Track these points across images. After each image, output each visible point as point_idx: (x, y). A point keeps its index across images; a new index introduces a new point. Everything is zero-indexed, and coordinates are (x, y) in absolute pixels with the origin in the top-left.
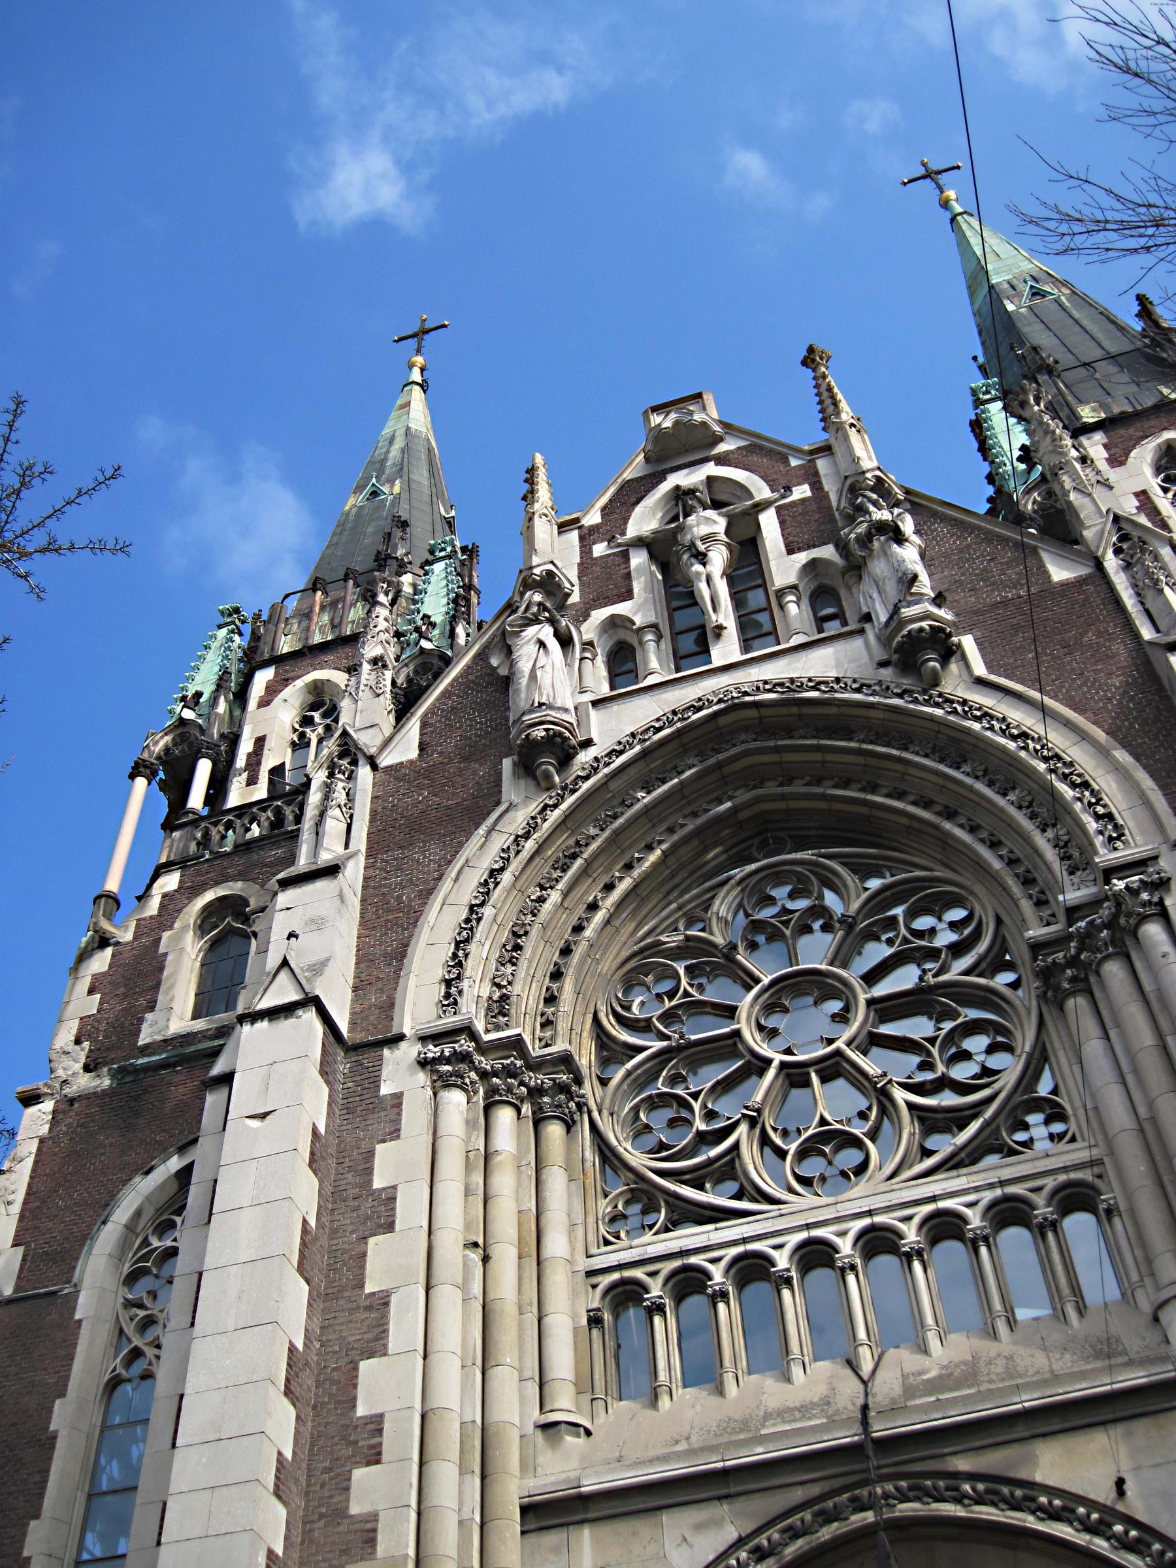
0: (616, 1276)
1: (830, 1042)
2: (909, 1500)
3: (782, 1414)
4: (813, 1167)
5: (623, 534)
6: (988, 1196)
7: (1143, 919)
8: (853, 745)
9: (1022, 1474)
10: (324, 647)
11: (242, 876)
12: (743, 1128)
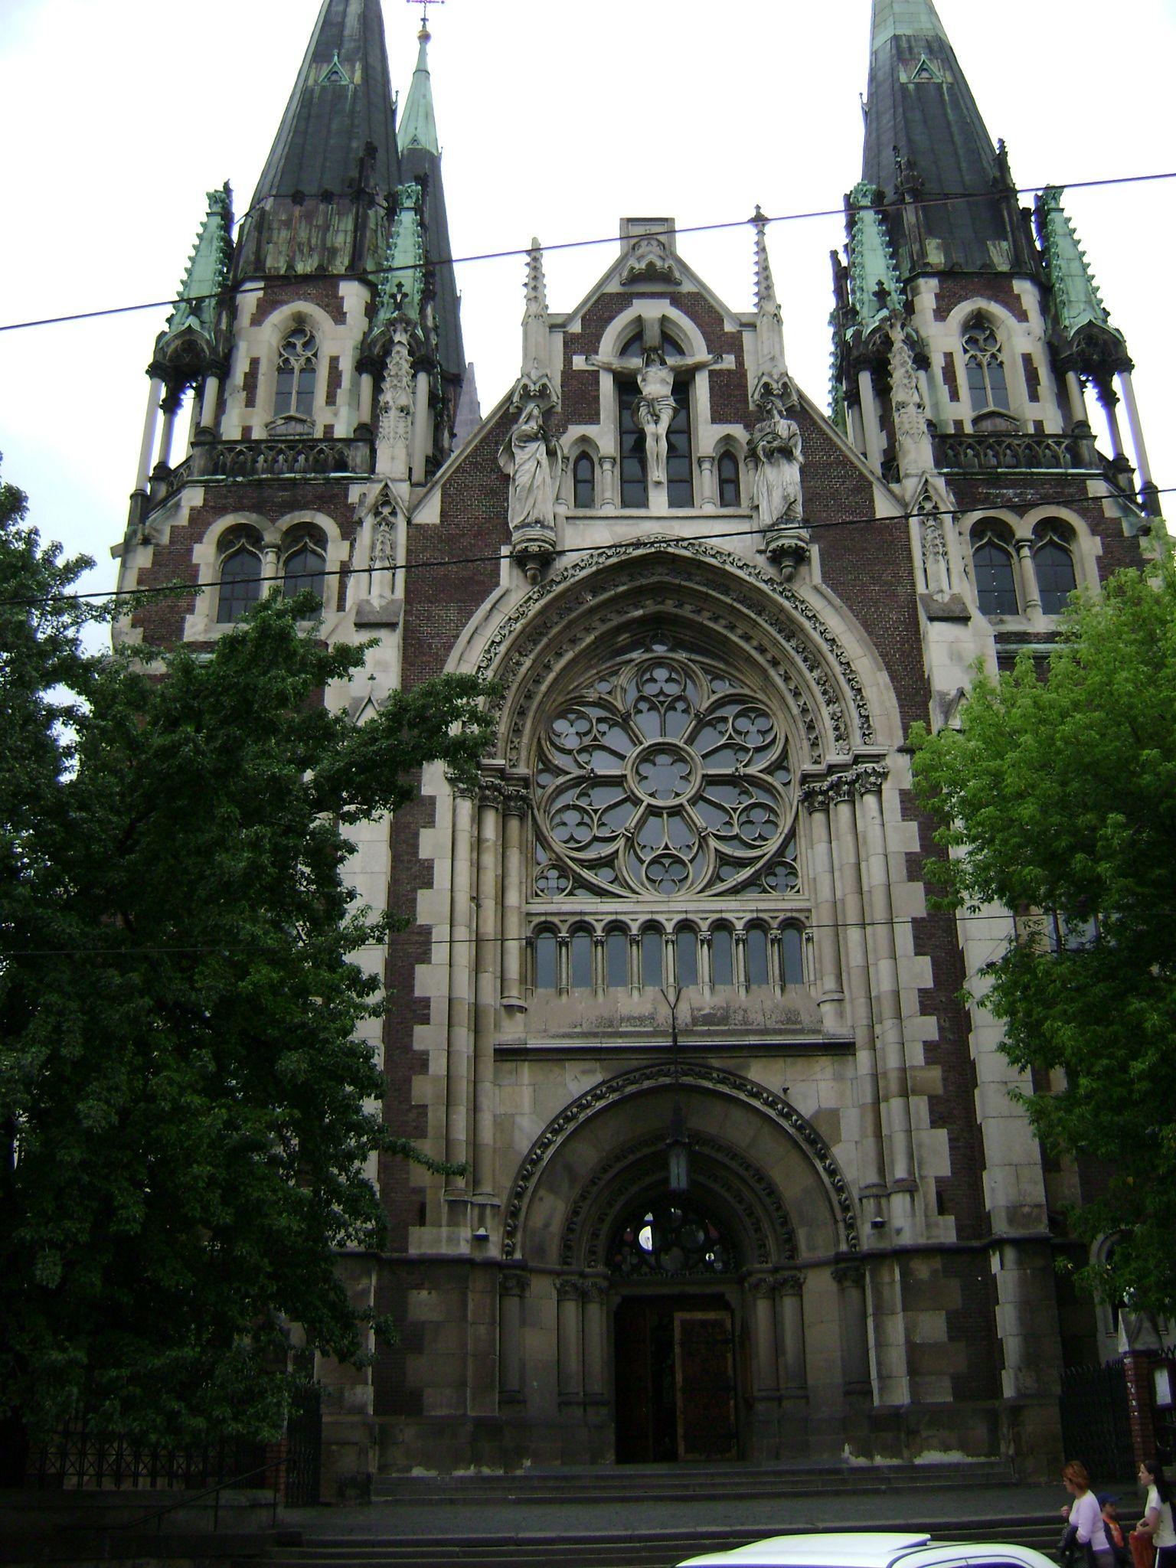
0: (543, 918)
1: (677, 795)
2: (687, 1075)
3: (630, 1019)
4: (657, 873)
5: (596, 353)
6: (749, 916)
7: (868, 791)
8: (728, 600)
9: (743, 1074)
10: (306, 278)
11: (254, 508)
12: (620, 843)
